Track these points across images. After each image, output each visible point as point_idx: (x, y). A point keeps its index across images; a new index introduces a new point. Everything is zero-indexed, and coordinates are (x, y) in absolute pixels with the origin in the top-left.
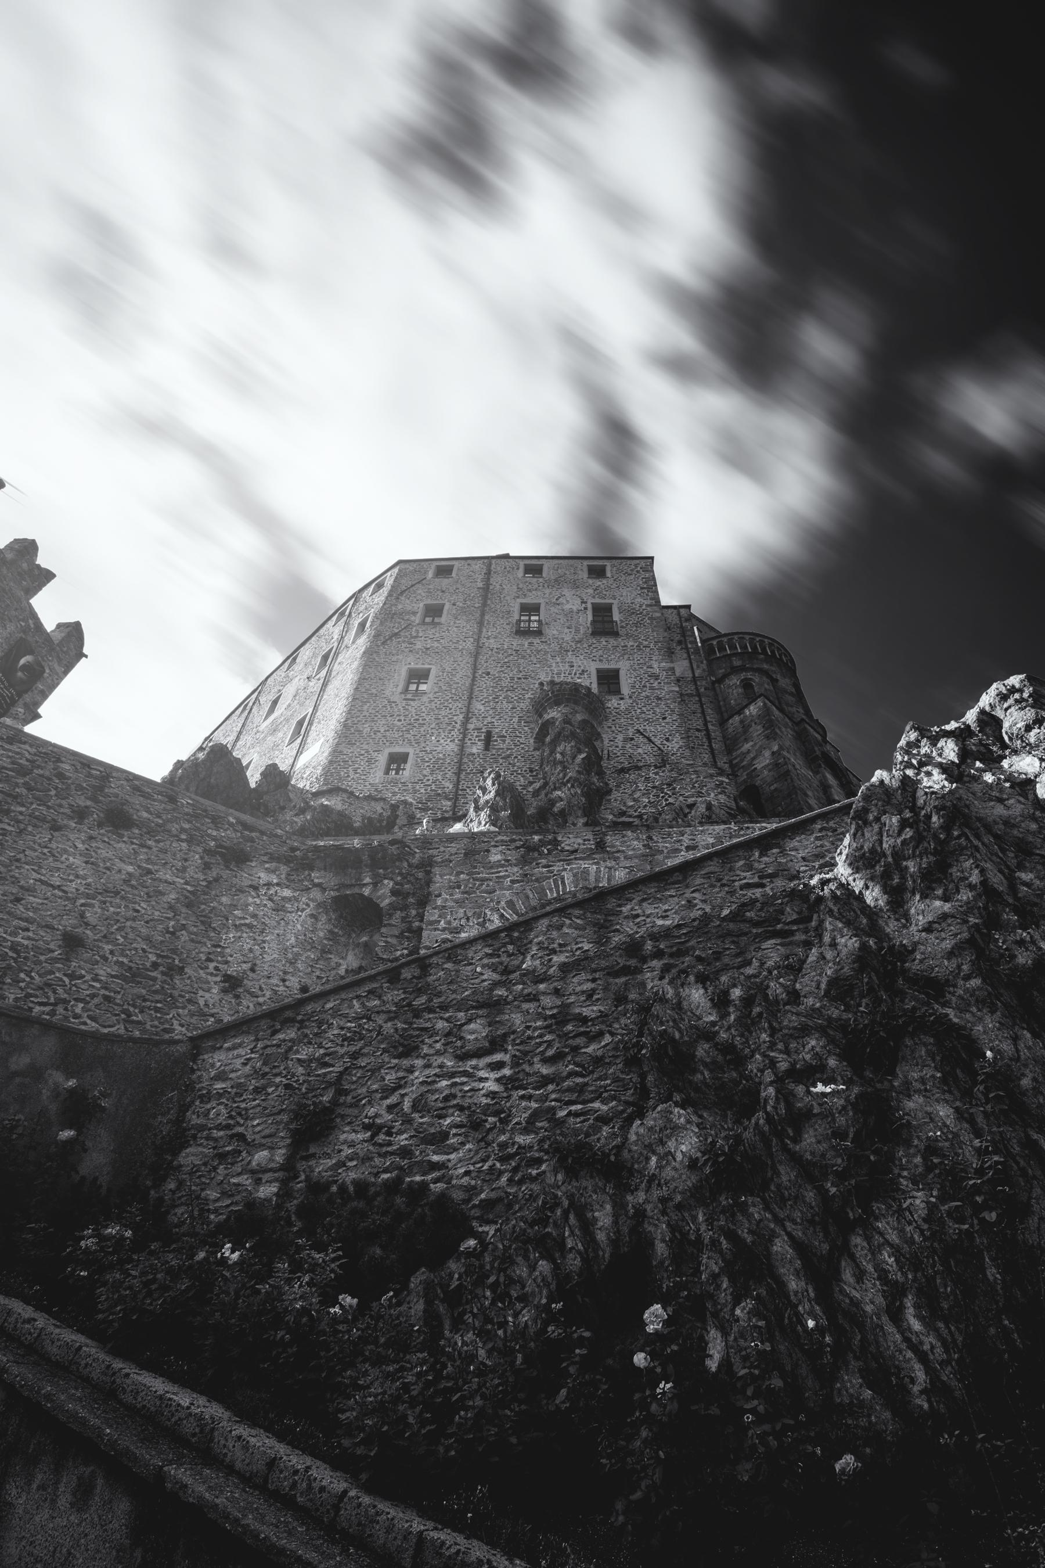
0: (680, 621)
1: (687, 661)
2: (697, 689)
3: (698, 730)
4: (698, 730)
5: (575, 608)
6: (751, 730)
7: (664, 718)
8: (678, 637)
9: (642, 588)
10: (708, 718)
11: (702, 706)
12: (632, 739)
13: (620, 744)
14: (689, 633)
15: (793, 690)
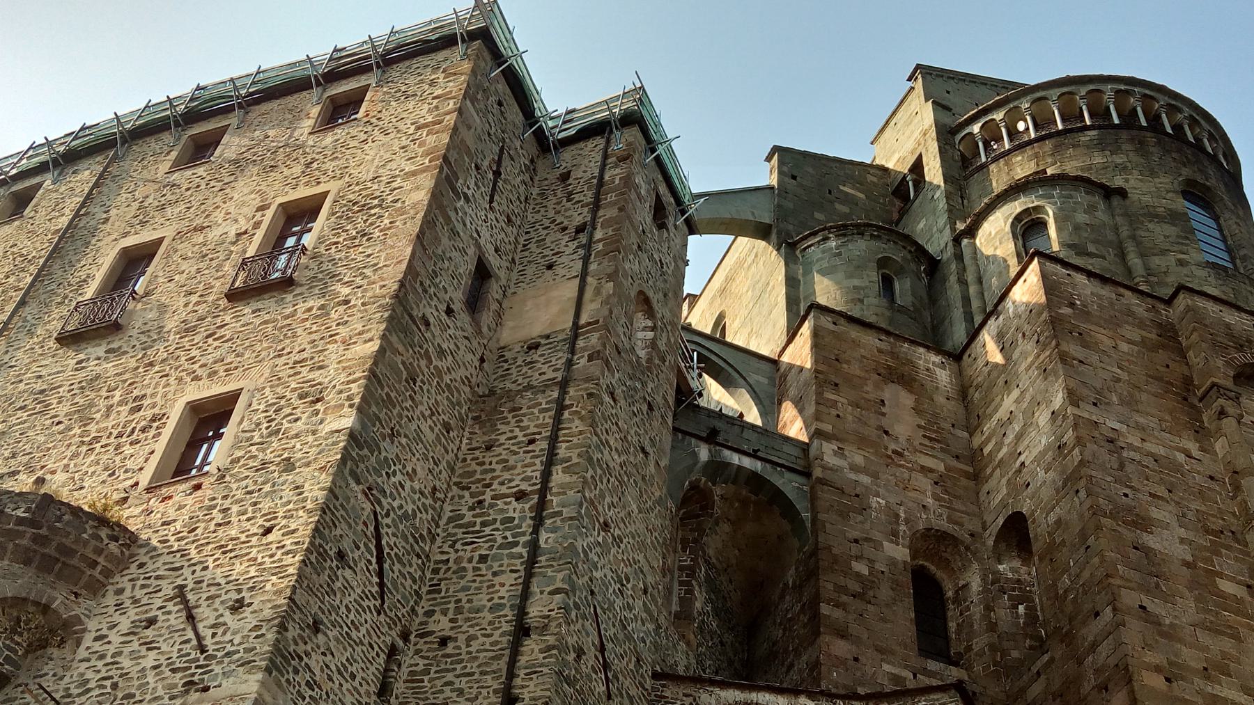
0: (603, 166)
1: (577, 281)
2: (570, 363)
3: (520, 496)
4: (520, 496)
5: (232, 233)
6: (1015, 356)
7: (268, 531)
8: (579, 216)
9: (418, 128)
10: (562, 451)
11: (561, 407)
12: (151, 622)
13: (112, 649)
14: (611, 197)
15: (1182, 204)
